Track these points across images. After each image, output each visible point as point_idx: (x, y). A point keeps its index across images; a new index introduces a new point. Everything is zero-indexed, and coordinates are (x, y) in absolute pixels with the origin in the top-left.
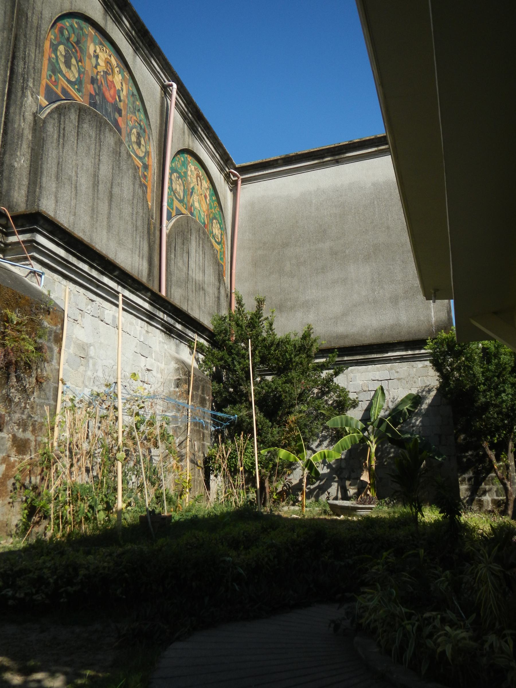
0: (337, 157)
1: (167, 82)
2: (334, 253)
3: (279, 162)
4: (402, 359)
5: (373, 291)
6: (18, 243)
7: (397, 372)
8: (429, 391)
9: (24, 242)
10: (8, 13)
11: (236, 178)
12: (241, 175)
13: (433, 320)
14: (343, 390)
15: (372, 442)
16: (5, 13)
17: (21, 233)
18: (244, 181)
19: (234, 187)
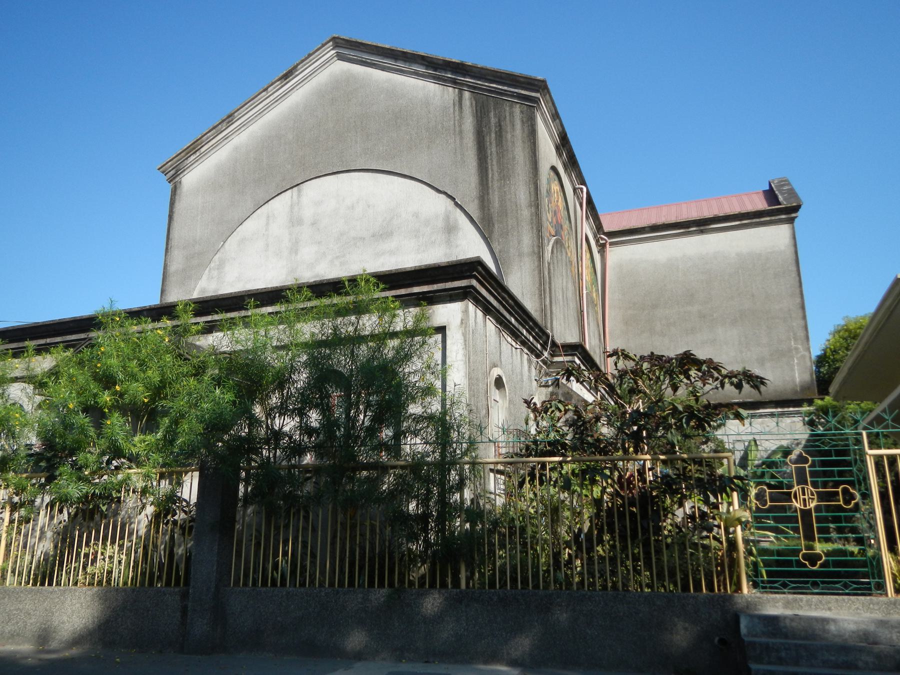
0: (702, 228)
1: (577, 186)
2: (702, 316)
3: (647, 229)
4: (772, 415)
5: (741, 352)
6: (563, 362)
7: (768, 426)
8: (798, 444)
9: (567, 362)
10: (533, 193)
11: (604, 242)
12: (609, 239)
13: (798, 380)
14: (722, 442)
15: (752, 487)
16: (530, 193)
17: (565, 355)
18: (611, 244)
19: (602, 248)
